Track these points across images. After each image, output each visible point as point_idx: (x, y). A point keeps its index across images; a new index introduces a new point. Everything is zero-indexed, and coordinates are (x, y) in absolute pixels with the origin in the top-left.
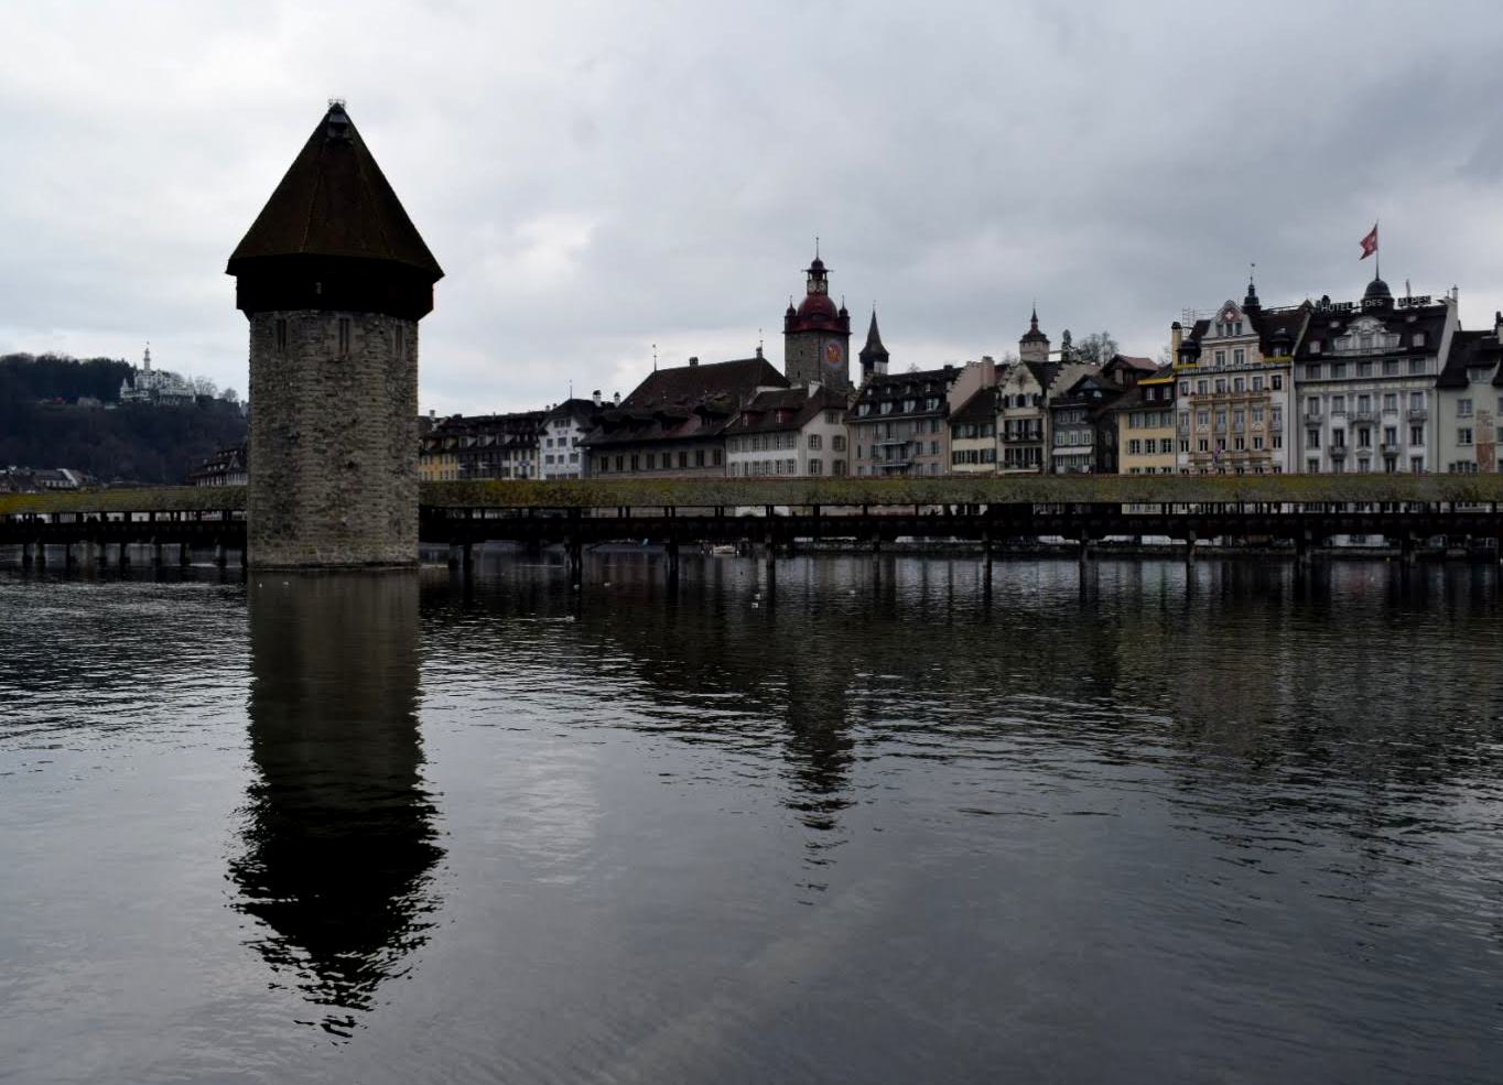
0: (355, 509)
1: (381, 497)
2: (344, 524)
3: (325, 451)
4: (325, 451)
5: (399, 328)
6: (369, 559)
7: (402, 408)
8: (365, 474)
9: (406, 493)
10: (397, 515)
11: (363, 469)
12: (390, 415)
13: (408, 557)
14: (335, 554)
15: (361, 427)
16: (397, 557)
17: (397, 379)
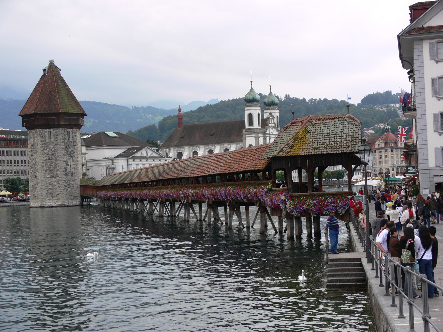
0: (37, 190)
1: (42, 186)
2: (35, 194)
3: (31, 173)
4: (31, 173)
5: (50, 133)
6: (40, 205)
7: (52, 157)
8: (39, 179)
9: (56, 184)
10: (50, 191)
11: (38, 178)
12: (46, 160)
13: (58, 204)
14: (34, 204)
15: (37, 165)
16: (51, 204)
17: (49, 148)
